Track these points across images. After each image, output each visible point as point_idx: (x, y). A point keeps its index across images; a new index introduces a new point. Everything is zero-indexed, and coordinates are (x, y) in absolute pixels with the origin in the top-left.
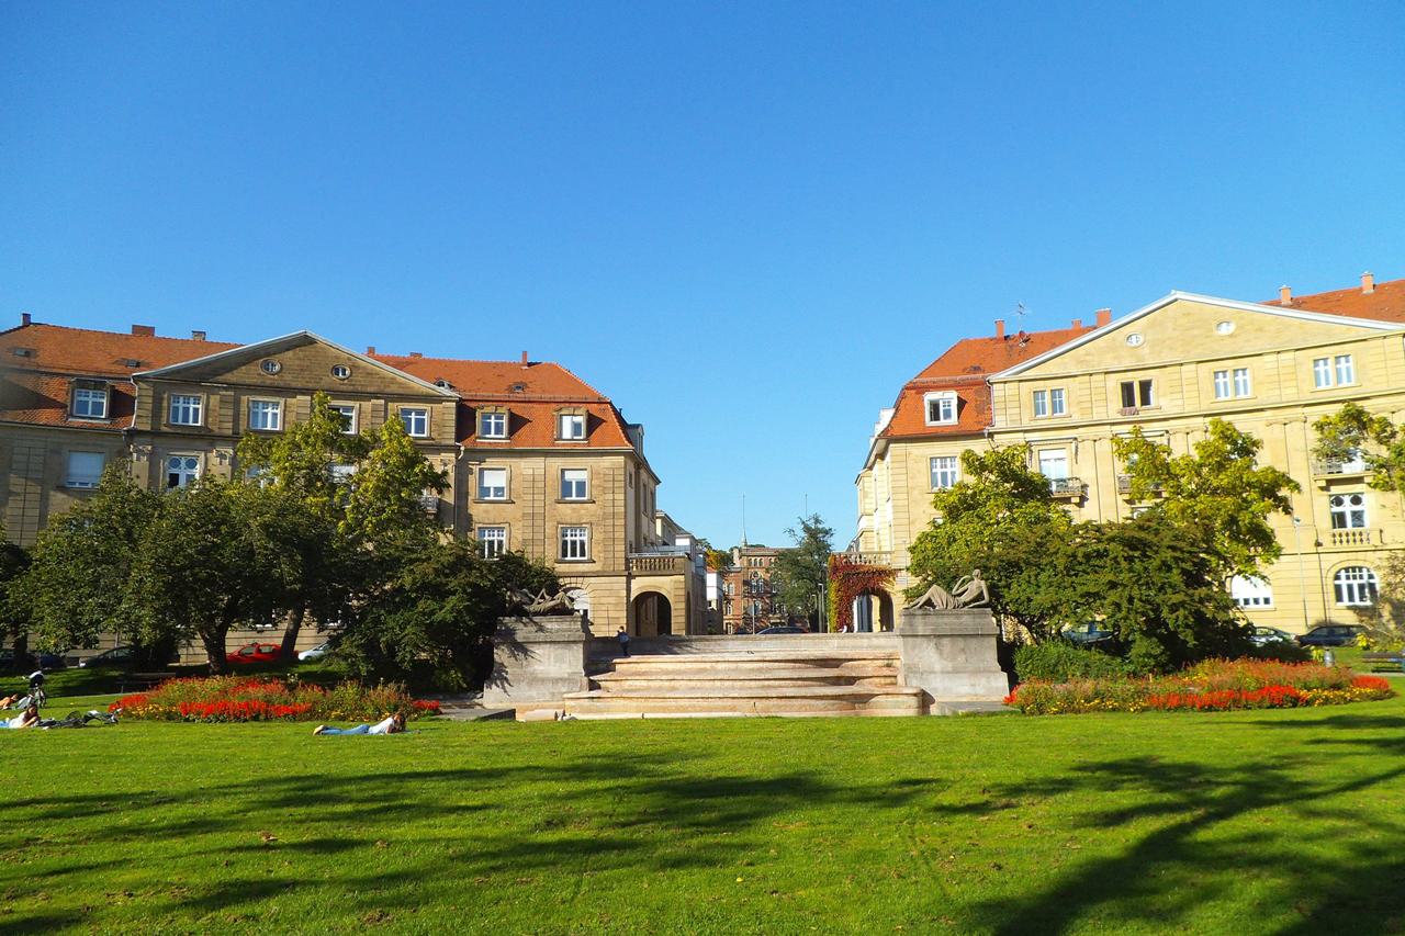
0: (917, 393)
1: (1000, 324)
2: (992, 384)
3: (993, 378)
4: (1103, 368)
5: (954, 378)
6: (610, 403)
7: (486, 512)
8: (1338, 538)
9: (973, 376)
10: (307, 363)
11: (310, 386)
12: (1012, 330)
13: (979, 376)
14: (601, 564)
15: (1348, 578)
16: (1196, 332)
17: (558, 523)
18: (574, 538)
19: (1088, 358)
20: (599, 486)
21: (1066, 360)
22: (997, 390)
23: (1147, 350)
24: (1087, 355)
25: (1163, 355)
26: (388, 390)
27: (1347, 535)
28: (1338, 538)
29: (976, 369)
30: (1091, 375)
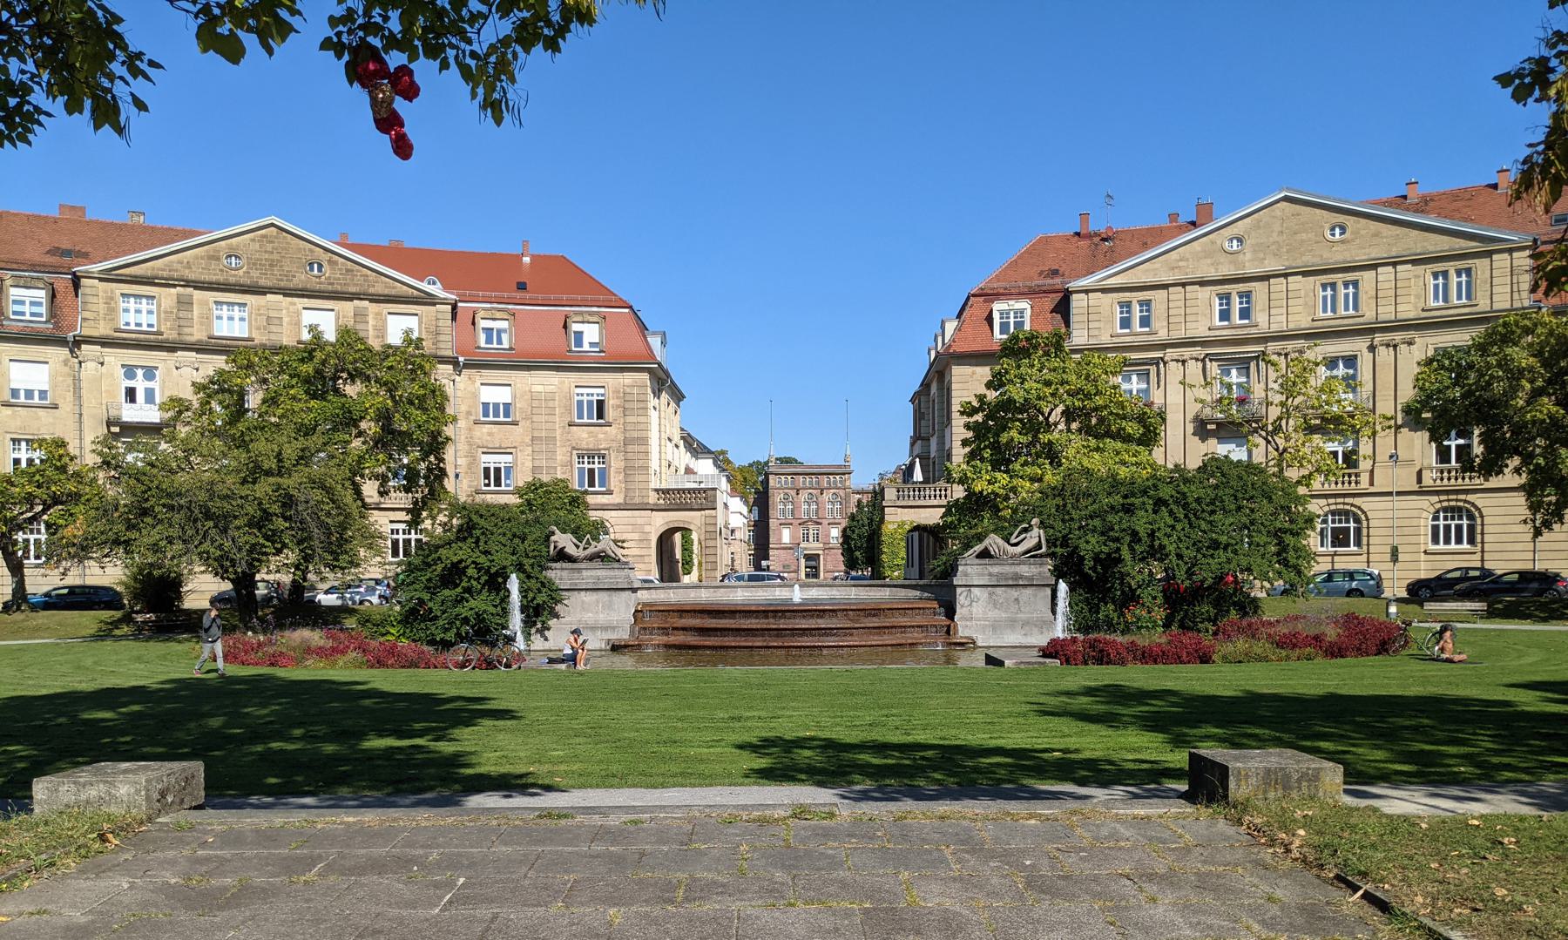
0: (985, 301)
1: (1084, 216)
2: (1072, 293)
3: (1073, 285)
4: (1198, 275)
5: (1028, 283)
6: (630, 307)
7: (490, 434)
8: (1445, 474)
9: (1051, 281)
10: (276, 256)
11: (282, 284)
12: (1097, 225)
13: (1058, 280)
14: (622, 496)
15: (1446, 518)
16: (1304, 236)
17: (574, 448)
18: (591, 466)
19: (1181, 264)
20: (618, 406)
21: (1157, 266)
22: (1078, 302)
23: (1248, 256)
24: (1181, 260)
25: (1266, 262)
26: (371, 290)
27: (1449, 472)
28: (1445, 474)
29: (1055, 273)
30: (1184, 285)
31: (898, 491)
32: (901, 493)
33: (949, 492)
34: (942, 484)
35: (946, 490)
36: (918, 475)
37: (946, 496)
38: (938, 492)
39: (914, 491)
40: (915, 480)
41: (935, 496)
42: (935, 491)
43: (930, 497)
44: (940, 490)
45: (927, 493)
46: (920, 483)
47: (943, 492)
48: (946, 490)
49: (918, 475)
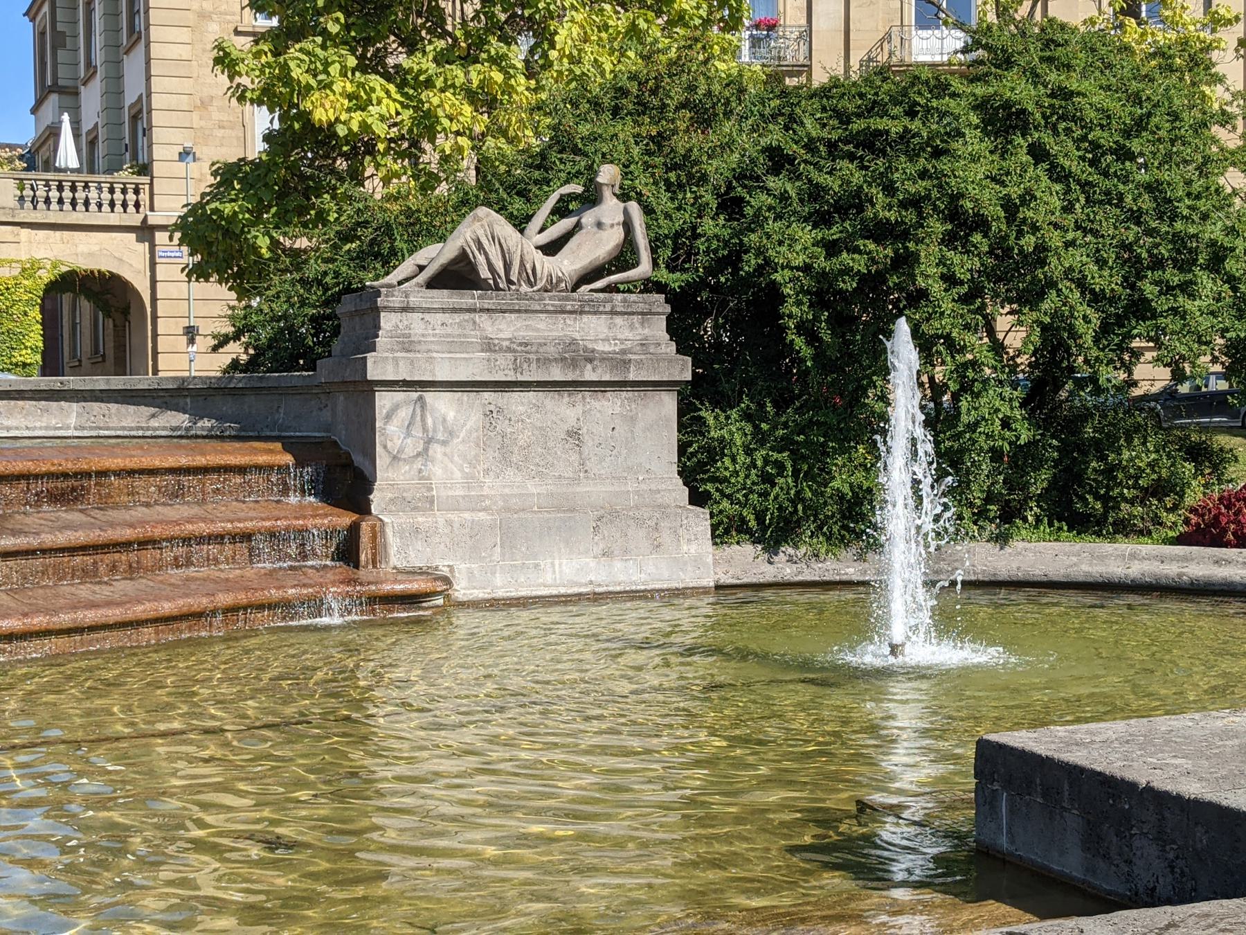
31: (22, 189)
32: (28, 192)
33: (144, 197)
34: (125, 176)
35: (137, 192)
36: (68, 153)
37: (137, 205)
38: (118, 196)
39: (60, 188)
40: (60, 162)
41: (112, 204)
42: (112, 191)
43: (100, 206)
44: (124, 191)
45: (93, 194)
46: (73, 171)
47: (131, 197)
48: (137, 192)
49: (68, 153)
